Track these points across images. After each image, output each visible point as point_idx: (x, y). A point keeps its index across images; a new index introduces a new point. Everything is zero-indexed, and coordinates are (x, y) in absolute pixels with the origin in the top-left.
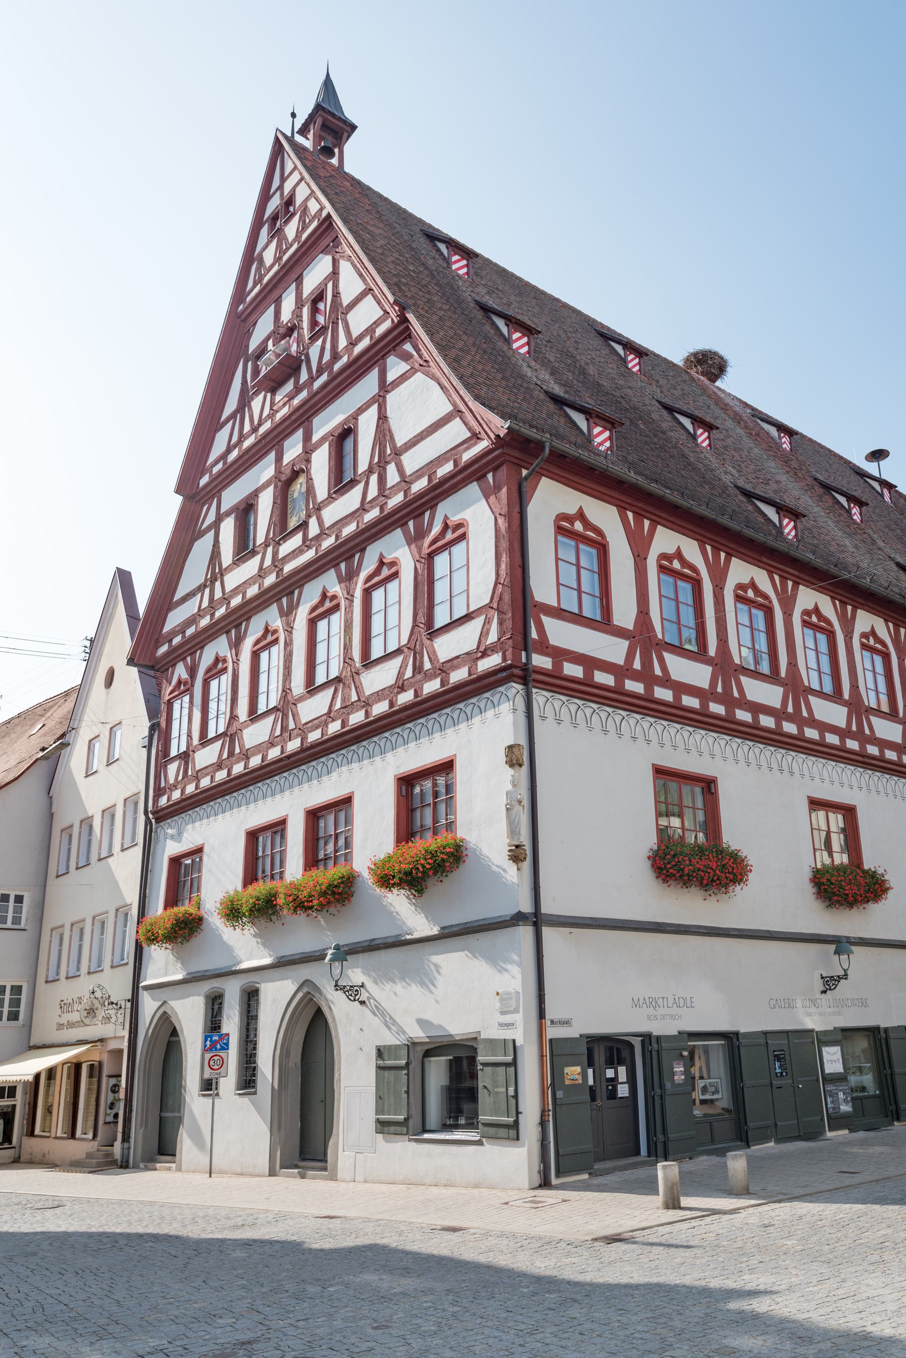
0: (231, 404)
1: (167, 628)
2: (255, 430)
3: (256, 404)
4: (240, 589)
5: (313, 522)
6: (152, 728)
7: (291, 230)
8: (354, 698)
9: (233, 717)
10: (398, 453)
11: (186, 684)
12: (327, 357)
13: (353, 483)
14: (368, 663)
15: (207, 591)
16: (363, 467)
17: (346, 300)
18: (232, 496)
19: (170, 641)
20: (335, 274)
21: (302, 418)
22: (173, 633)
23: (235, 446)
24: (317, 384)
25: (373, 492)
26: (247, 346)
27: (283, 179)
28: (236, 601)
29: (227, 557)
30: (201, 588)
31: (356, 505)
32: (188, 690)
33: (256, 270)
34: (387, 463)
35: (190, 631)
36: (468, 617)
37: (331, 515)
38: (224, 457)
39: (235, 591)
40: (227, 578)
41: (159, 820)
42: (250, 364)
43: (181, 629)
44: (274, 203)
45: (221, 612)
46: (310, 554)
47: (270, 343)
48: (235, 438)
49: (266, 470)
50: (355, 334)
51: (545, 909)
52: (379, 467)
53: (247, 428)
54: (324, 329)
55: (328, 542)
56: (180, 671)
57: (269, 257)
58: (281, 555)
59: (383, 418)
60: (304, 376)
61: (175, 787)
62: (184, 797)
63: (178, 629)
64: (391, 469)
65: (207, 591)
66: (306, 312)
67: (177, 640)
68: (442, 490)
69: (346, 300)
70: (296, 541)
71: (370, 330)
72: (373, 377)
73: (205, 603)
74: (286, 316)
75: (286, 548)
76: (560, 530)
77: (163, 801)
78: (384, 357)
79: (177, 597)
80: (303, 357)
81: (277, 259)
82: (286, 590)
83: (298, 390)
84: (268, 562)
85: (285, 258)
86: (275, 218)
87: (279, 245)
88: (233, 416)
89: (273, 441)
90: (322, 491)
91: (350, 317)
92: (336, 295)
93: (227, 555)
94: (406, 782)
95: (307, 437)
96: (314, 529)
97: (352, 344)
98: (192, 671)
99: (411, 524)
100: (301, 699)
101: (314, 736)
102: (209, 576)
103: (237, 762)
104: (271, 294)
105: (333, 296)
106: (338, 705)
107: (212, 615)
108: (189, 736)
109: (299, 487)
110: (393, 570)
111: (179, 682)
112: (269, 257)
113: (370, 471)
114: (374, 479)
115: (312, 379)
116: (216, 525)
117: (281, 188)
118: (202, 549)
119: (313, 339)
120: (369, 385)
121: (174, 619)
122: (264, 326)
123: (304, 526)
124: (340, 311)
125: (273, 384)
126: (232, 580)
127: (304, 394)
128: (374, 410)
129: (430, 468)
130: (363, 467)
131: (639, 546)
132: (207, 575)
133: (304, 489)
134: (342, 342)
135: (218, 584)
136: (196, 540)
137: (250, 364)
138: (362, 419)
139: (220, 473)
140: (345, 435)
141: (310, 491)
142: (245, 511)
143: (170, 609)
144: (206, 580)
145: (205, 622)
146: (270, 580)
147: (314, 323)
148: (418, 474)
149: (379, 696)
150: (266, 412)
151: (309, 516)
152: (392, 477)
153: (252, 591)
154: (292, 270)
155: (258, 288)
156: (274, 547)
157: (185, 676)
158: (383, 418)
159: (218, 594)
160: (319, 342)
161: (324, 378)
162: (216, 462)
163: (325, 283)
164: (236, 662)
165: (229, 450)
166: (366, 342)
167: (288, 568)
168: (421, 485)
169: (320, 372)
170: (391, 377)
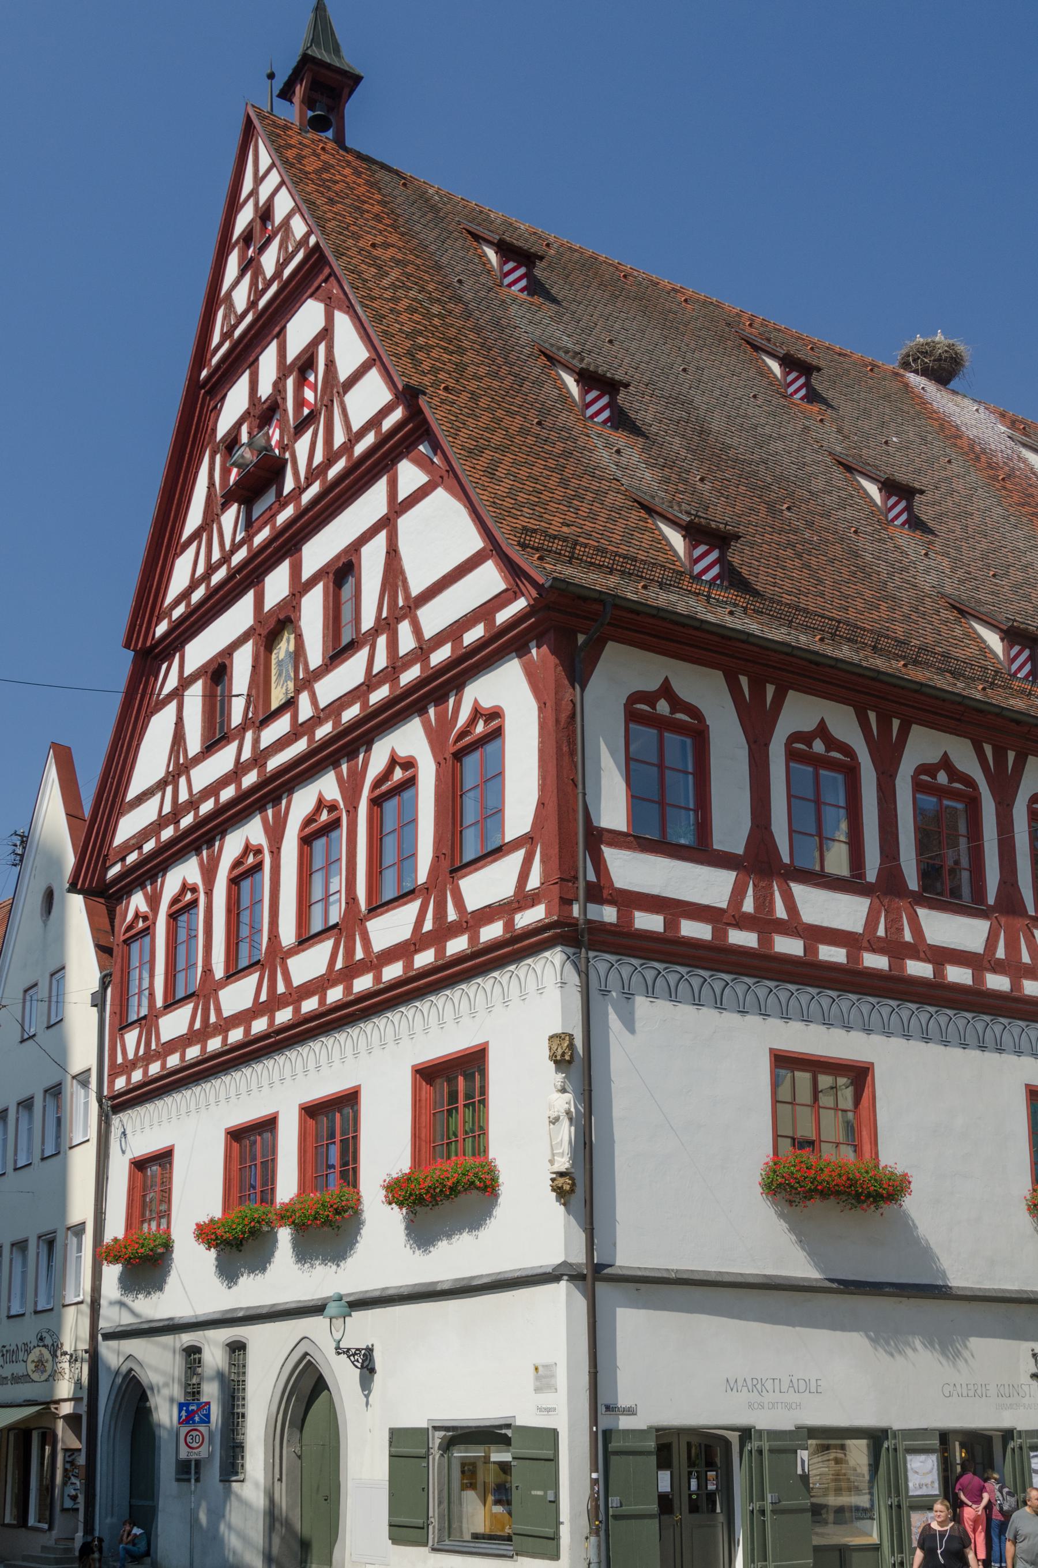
0: (194, 519)
1: (118, 841)
2: (225, 559)
4: (213, 790)
5: (304, 699)
6: (104, 985)
7: (269, 261)
9: (208, 970)
11: (145, 918)
12: (319, 458)
13: (353, 647)
14: (377, 908)
15: (169, 790)
16: (367, 622)
17: (344, 373)
18: (199, 651)
20: (326, 334)
21: (288, 544)
22: (128, 847)
24: (306, 497)
26: (214, 430)
27: (258, 180)
29: (194, 745)
30: (161, 786)
31: (359, 678)
32: (148, 928)
33: (225, 317)
34: (399, 620)
35: (149, 846)
36: (499, 852)
38: (185, 595)
41: (117, 1109)
42: (218, 457)
43: (136, 842)
44: (245, 217)
46: (301, 746)
47: (244, 429)
48: (201, 570)
49: (240, 616)
50: (356, 427)
52: (387, 625)
53: (216, 555)
54: (312, 418)
55: (324, 731)
56: (138, 901)
57: (240, 298)
58: (263, 745)
59: (393, 553)
60: (289, 485)
61: (132, 1065)
62: (147, 1080)
63: (133, 842)
64: (404, 628)
65: (169, 790)
66: (290, 382)
67: (132, 858)
69: (344, 373)
70: (281, 726)
71: (374, 422)
72: (378, 491)
74: (265, 390)
75: (271, 734)
76: (632, 716)
77: (120, 1083)
78: (395, 461)
79: (131, 795)
80: (287, 455)
81: (252, 304)
82: (271, 793)
83: (282, 503)
85: (262, 303)
86: (247, 238)
87: (254, 283)
88: (196, 535)
89: (249, 577)
90: (315, 657)
91: (350, 398)
92: (330, 363)
94: (427, 1074)
95: (296, 570)
96: (305, 711)
97: (354, 438)
98: (153, 902)
99: (432, 711)
100: (293, 951)
102: (171, 769)
103: (213, 1036)
104: (243, 356)
108: (152, 995)
109: (285, 646)
110: (409, 773)
111: (137, 915)
112: (240, 298)
113: (375, 632)
114: (382, 641)
115: (299, 490)
116: (178, 694)
117: (254, 193)
118: (160, 728)
119: (300, 429)
120: (372, 503)
121: (128, 827)
122: (236, 402)
123: (290, 704)
124: (336, 389)
127: (289, 512)
128: (382, 537)
129: (454, 632)
131: (757, 726)
132: (168, 766)
133: (292, 648)
134: (339, 438)
135: (183, 781)
136: (152, 714)
137: (218, 457)
138: (366, 550)
139: (183, 619)
140: (343, 571)
141: (299, 653)
142: (217, 672)
143: (121, 814)
144: (168, 773)
147: (300, 402)
148: (438, 641)
149: (390, 955)
151: (298, 691)
152: (407, 643)
153: (227, 794)
154: (269, 323)
155: (227, 345)
156: (254, 733)
157: (144, 908)
158: (393, 553)
160: (308, 436)
161: (315, 489)
162: (177, 603)
163: (314, 343)
164: (209, 893)
166: (369, 439)
167: (273, 763)
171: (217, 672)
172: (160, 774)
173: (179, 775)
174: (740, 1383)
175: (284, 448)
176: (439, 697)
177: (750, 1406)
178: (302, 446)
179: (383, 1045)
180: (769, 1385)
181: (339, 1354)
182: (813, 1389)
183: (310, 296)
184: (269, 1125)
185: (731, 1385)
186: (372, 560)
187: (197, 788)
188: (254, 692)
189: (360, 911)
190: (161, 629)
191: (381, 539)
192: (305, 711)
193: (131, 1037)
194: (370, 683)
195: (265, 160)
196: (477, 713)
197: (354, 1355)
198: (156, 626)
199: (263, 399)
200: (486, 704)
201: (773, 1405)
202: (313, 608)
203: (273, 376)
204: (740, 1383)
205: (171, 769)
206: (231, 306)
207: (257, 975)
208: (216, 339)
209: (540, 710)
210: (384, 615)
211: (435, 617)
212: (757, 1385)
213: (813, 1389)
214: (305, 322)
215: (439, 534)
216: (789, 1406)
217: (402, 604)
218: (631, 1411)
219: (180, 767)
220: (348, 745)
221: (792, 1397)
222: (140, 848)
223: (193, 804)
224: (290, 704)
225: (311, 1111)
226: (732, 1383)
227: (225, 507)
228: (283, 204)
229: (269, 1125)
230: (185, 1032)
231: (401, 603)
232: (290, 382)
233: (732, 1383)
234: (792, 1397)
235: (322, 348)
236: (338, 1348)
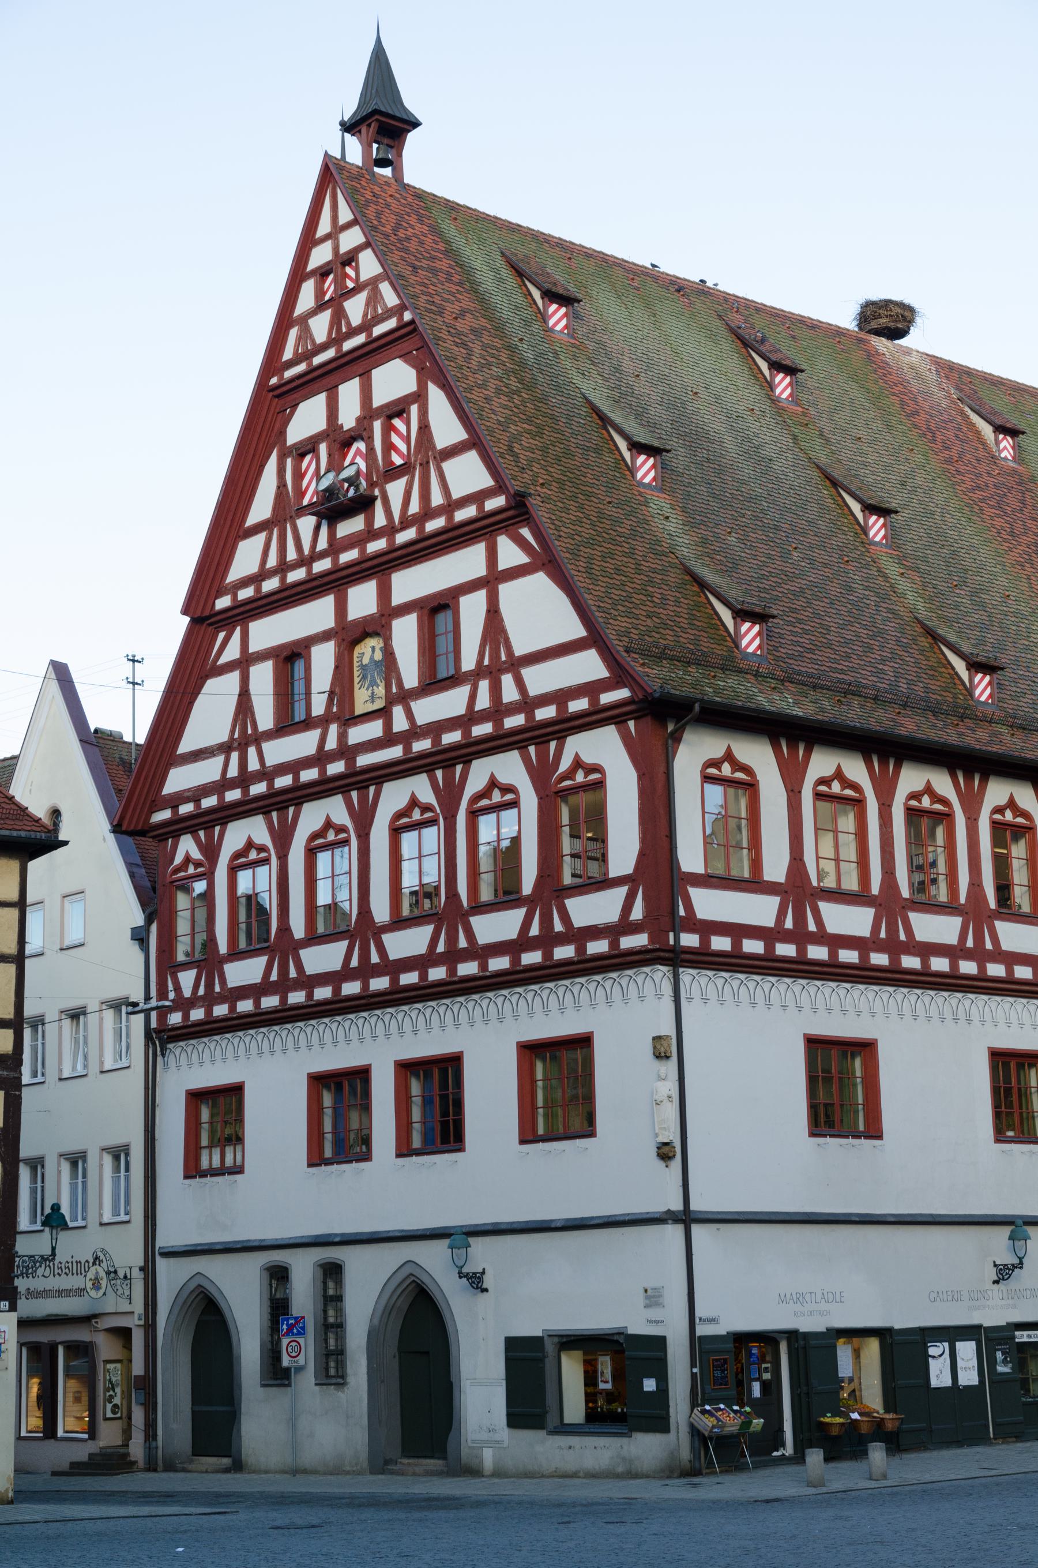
3: (306, 524)
4: (293, 767)
5: (398, 712)
8: (463, 943)
10: (517, 664)
15: (235, 756)
16: (468, 664)
19: (175, 808)
21: (380, 568)
23: (272, 573)
25: (483, 701)
27: (338, 229)
28: (283, 782)
30: (225, 749)
33: (299, 339)
34: (502, 671)
35: (210, 802)
37: (431, 709)
38: (256, 579)
39: (283, 769)
40: (266, 746)
43: (197, 794)
45: (258, 789)
46: (396, 752)
48: (272, 562)
49: (317, 615)
51: (694, 1207)
52: (490, 671)
53: (292, 555)
55: (422, 745)
57: (320, 327)
59: (493, 613)
60: (380, 520)
63: (189, 794)
64: (507, 681)
65: (235, 756)
68: (569, 725)
73: (233, 772)
80: (377, 492)
82: (361, 783)
84: (331, 744)
92: (425, 427)
93: (265, 717)
96: (400, 723)
101: (410, 978)
102: (236, 736)
104: (323, 379)
105: (420, 428)
106: (441, 948)
107: (246, 791)
119: (392, 473)
121: (179, 779)
125: (333, 508)
126: (279, 751)
128: (481, 595)
130: (468, 664)
132: (233, 731)
135: (252, 751)
145: (233, 795)
146: (336, 768)
150: (322, 544)
153: (309, 775)
156: (339, 727)
158: (493, 613)
159: (253, 765)
162: (244, 583)
164: (283, 858)
165: (262, 575)
167: (364, 760)
168: (546, 713)
169: (406, 523)
170: (501, 566)
171: (291, 657)
172: (224, 737)
173: (247, 745)
174: (788, 1296)
175: (372, 485)
176: (541, 742)
177: (795, 1314)
178: (396, 489)
179: (486, 1022)
180: (808, 1297)
181: (460, 1277)
182: (838, 1300)
183: (400, 357)
184: (362, 1075)
185: (782, 1299)
186: (472, 610)
187: (271, 761)
188: (337, 690)
189: (462, 906)
190: (223, 602)
191: (481, 595)
192: (400, 723)
193: (187, 979)
194: (471, 717)
195: (345, 215)
196: (578, 763)
197: (471, 1278)
198: (216, 598)
199: (345, 428)
200: (588, 759)
201: (811, 1313)
202: (405, 633)
203: (356, 412)
204: (788, 1296)
205: (236, 736)
206: (306, 332)
207: (346, 943)
208: (288, 354)
209: (639, 778)
210: (486, 662)
211: (541, 679)
212: (799, 1298)
213: (838, 1300)
214: (394, 379)
215: (539, 612)
216: (821, 1313)
217: (501, 658)
218: (714, 1321)
219: (245, 736)
220: (447, 761)
221: (823, 1306)
222: (197, 801)
223: (267, 774)
224: (384, 713)
225: (406, 1069)
226: (782, 1296)
227: (302, 511)
228: (369, 265)
229: (362, 1075)
230: (259, 981)
231: (503, 658)
232: (377, 425)
233: (782, 1296)
234: (823, 1306)
235: (414, 409)
236: (460, 1273)
